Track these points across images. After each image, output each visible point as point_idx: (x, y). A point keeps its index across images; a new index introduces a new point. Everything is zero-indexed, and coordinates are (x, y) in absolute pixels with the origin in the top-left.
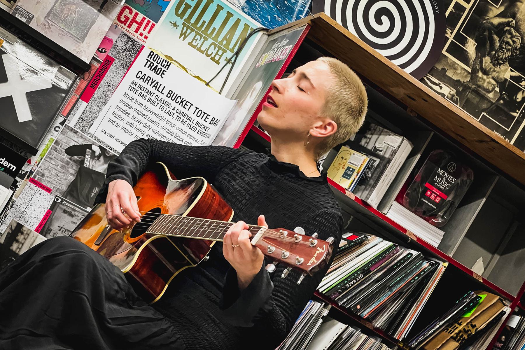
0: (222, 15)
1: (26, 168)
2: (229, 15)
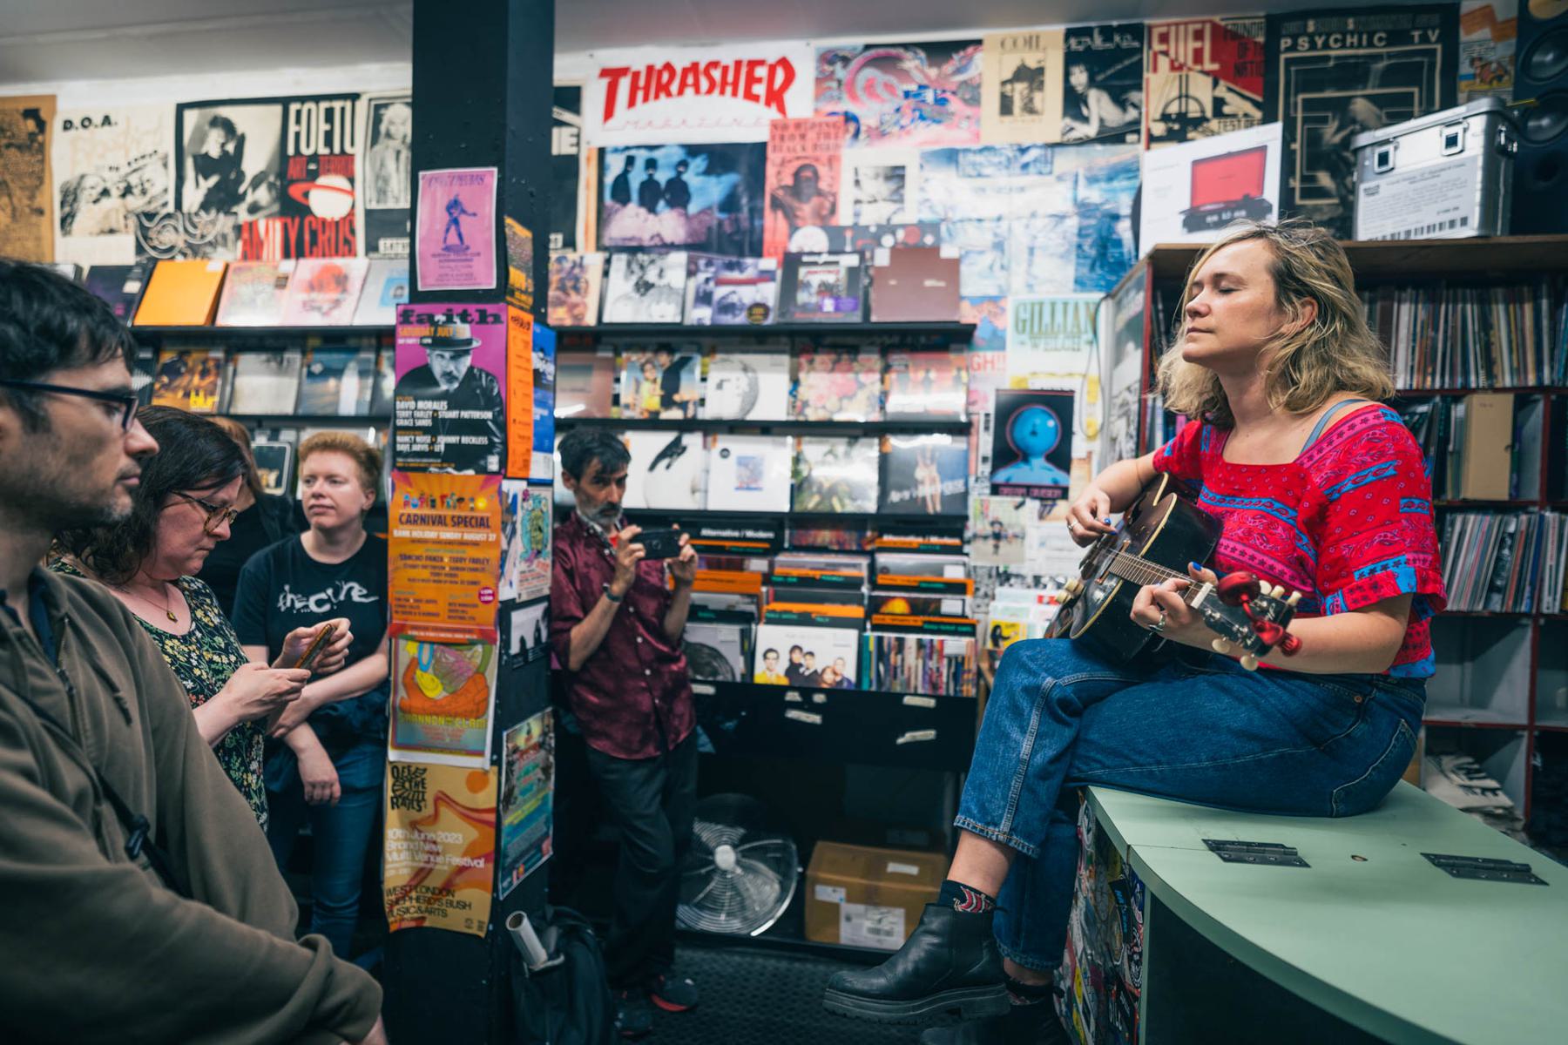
0: (1059, 308)
1: (968, 534)
2: (1065, 304)
